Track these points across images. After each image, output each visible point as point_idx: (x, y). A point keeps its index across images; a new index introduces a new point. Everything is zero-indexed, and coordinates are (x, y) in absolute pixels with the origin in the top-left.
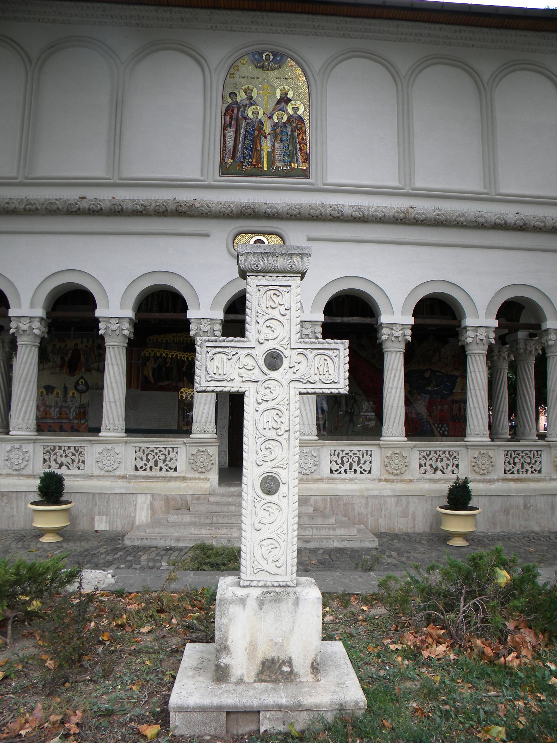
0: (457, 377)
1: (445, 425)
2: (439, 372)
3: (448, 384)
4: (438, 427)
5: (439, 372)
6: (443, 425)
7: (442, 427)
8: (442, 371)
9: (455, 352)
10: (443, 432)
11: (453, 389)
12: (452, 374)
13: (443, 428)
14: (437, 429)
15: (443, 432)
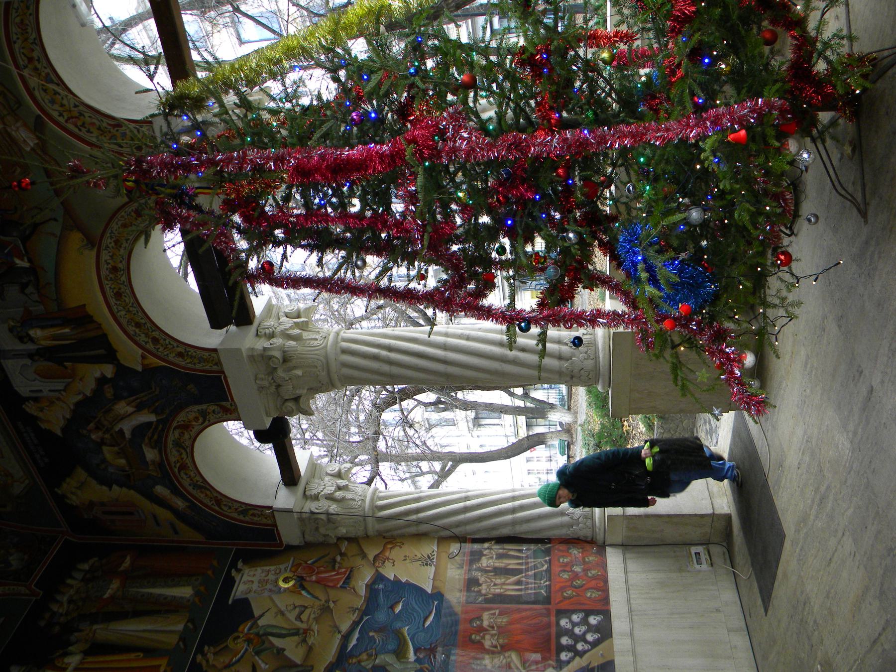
0: (379, 578)
1: (564, 622)
2: (346, 637)
3: (398, 609)
4: (571, 648)
5: (346, 637)
6: (562, 632)
7: (570, 633)
8: (345, 627)
9: (286, 580)
10: (591, 629)
11: (421, 591)
12: (362, 591)
13: (577, 630)
14: (581, 654)
15: (591, 629)
